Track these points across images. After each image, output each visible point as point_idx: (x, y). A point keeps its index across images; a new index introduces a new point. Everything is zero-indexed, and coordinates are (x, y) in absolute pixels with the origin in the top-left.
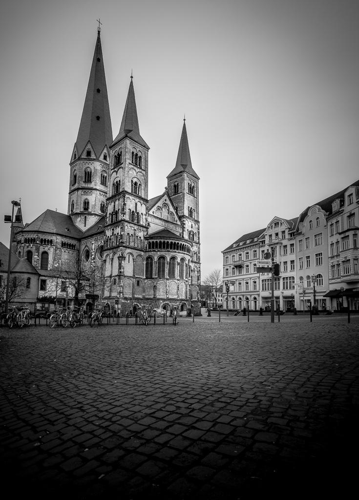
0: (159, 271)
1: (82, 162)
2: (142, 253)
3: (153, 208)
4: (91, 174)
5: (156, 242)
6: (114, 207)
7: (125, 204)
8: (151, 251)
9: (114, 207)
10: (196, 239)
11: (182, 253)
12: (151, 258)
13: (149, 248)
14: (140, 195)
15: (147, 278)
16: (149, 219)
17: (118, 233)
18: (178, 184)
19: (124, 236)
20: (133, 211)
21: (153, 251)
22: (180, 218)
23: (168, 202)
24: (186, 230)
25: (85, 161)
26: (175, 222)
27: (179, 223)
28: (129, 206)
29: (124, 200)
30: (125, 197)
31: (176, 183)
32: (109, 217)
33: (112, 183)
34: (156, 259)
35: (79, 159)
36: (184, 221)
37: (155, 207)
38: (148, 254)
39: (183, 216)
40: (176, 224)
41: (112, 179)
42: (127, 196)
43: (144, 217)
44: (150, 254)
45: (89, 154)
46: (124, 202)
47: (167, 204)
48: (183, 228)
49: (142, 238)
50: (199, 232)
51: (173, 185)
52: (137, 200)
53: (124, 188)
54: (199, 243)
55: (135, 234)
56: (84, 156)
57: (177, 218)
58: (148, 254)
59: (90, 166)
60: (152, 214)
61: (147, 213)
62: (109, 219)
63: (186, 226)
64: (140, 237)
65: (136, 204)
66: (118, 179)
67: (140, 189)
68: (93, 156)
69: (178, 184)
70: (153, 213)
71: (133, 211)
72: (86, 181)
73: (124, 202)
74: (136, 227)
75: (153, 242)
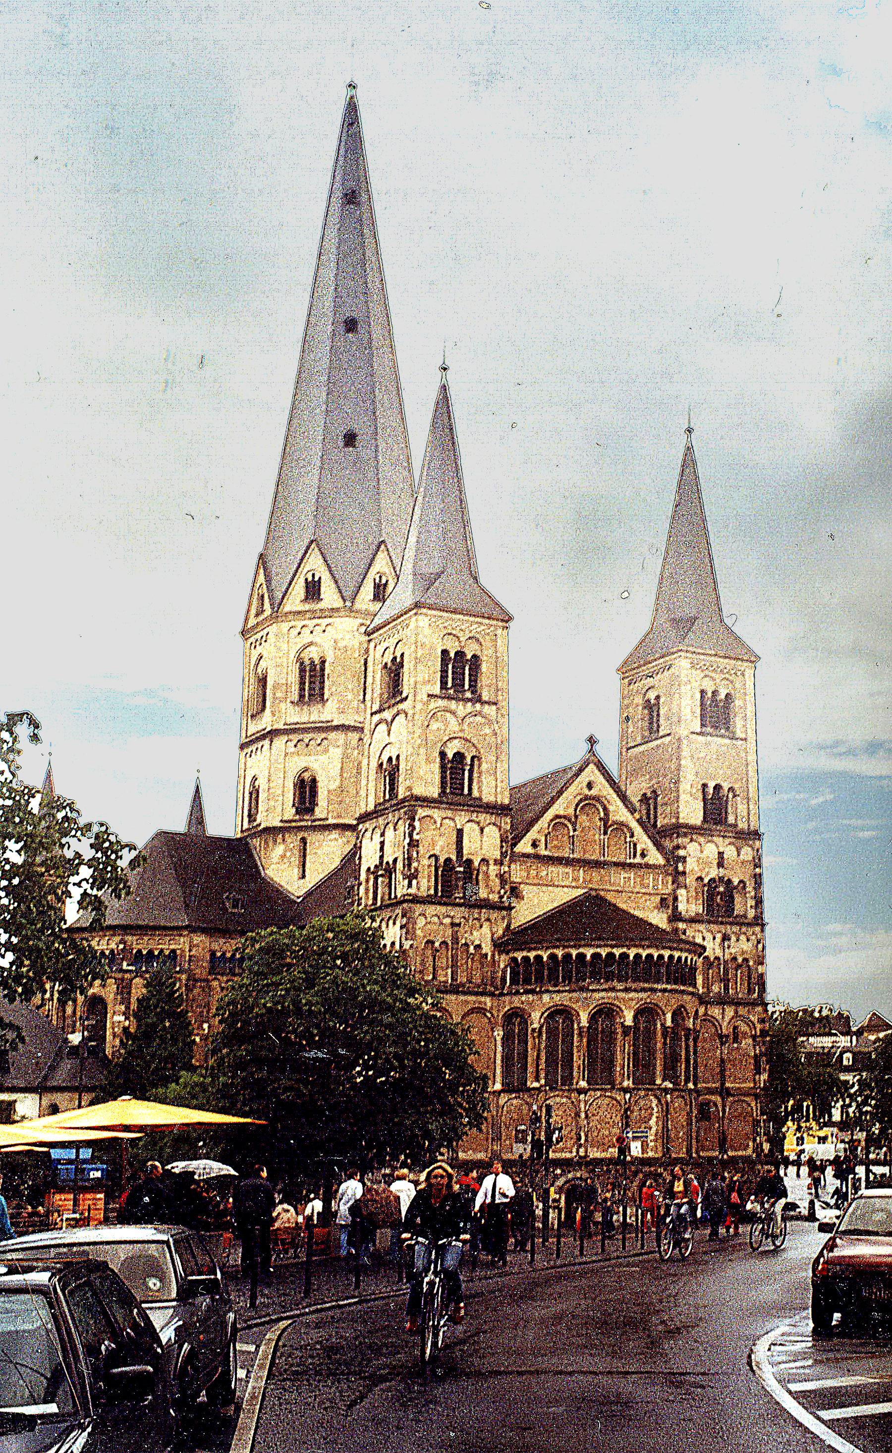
0: (551, 1062)
1: (285, 626)
2: (488, 1001)
3: (536, 828)
4: (323, 670)
5: (538, 958)
6: (382, 849)
7: (413, 844)
8: (517, 993)
9: (382, 849)
10: (743, 906)
11: (644, 990)
12: (522, 1017)
13: (514, 981)
14: (475, 794)
15: (508, 1088)
16: (517, 873)
17: (393, 944)
18: (658, 698)
19: (411, 953)
20: (448, 860)
21: (527, 992)
22: (658, 835)
23: (602, 788)
24: (690, 880)
25: (300, 624)
26: (638, 860)
27: (655, 857)
28: (433, 843)
29: (412, 827)
30: (413, 819)
31: (652, 695)
32: (367, 881)
33: (374, 764)
34: (536, 1019)
35: (276, 616)
36: (678, 847)
37: (543, 822)
38: (508, 1003)
39: (678, 829)
40: (648, 866)
41: (375, 750)
42: (421, 812)
43: (493, 870)
44: (517, 1001)
45: (313, 590)
46: (411, 836)
47: (597, 799)
48: (678, 876)
49: (487, 948)
50: (758, 879)
51: (639, 700)
52: (461, 819)
53: (409, 788)
54: (759, 921)
55: (456, 940)
56: (296, 599)
57: (643, 841)
58: (508, 1003)
59: (318, 637)
60: (529, 850)
61: (503, 855)
62: (367, 890)
63: (691, 865)
64: (478, 947)
65: (460, 833)
66: (392, 752)
67: (475, 775)
68: (329, 596)
69: (658, 698)
70: (535, 845)
71: (448, 860)
72: (302, 696)
73: (411, 836)
74: (458, 913)
75: (525, 959)
